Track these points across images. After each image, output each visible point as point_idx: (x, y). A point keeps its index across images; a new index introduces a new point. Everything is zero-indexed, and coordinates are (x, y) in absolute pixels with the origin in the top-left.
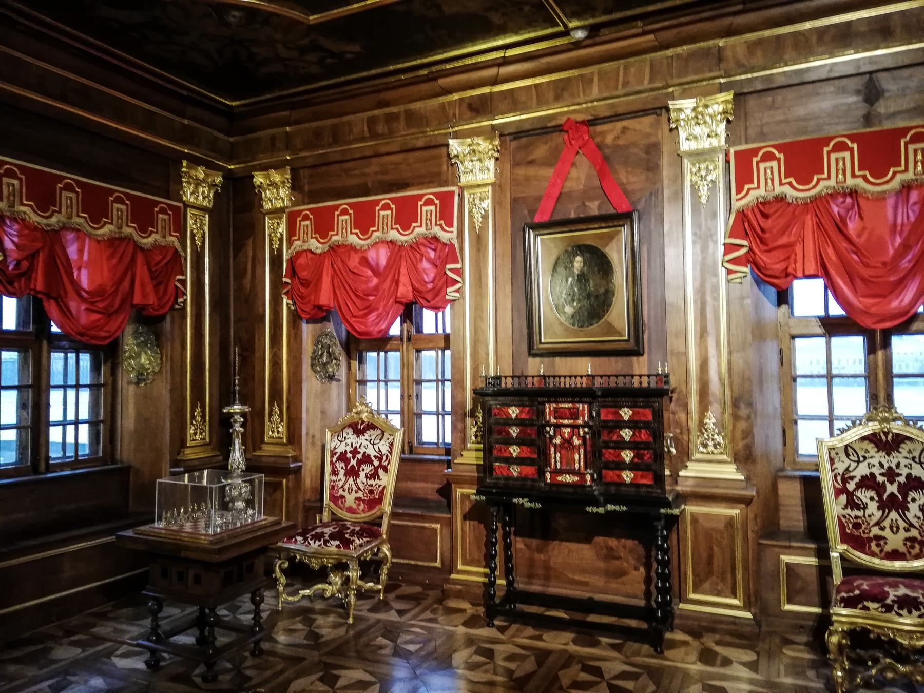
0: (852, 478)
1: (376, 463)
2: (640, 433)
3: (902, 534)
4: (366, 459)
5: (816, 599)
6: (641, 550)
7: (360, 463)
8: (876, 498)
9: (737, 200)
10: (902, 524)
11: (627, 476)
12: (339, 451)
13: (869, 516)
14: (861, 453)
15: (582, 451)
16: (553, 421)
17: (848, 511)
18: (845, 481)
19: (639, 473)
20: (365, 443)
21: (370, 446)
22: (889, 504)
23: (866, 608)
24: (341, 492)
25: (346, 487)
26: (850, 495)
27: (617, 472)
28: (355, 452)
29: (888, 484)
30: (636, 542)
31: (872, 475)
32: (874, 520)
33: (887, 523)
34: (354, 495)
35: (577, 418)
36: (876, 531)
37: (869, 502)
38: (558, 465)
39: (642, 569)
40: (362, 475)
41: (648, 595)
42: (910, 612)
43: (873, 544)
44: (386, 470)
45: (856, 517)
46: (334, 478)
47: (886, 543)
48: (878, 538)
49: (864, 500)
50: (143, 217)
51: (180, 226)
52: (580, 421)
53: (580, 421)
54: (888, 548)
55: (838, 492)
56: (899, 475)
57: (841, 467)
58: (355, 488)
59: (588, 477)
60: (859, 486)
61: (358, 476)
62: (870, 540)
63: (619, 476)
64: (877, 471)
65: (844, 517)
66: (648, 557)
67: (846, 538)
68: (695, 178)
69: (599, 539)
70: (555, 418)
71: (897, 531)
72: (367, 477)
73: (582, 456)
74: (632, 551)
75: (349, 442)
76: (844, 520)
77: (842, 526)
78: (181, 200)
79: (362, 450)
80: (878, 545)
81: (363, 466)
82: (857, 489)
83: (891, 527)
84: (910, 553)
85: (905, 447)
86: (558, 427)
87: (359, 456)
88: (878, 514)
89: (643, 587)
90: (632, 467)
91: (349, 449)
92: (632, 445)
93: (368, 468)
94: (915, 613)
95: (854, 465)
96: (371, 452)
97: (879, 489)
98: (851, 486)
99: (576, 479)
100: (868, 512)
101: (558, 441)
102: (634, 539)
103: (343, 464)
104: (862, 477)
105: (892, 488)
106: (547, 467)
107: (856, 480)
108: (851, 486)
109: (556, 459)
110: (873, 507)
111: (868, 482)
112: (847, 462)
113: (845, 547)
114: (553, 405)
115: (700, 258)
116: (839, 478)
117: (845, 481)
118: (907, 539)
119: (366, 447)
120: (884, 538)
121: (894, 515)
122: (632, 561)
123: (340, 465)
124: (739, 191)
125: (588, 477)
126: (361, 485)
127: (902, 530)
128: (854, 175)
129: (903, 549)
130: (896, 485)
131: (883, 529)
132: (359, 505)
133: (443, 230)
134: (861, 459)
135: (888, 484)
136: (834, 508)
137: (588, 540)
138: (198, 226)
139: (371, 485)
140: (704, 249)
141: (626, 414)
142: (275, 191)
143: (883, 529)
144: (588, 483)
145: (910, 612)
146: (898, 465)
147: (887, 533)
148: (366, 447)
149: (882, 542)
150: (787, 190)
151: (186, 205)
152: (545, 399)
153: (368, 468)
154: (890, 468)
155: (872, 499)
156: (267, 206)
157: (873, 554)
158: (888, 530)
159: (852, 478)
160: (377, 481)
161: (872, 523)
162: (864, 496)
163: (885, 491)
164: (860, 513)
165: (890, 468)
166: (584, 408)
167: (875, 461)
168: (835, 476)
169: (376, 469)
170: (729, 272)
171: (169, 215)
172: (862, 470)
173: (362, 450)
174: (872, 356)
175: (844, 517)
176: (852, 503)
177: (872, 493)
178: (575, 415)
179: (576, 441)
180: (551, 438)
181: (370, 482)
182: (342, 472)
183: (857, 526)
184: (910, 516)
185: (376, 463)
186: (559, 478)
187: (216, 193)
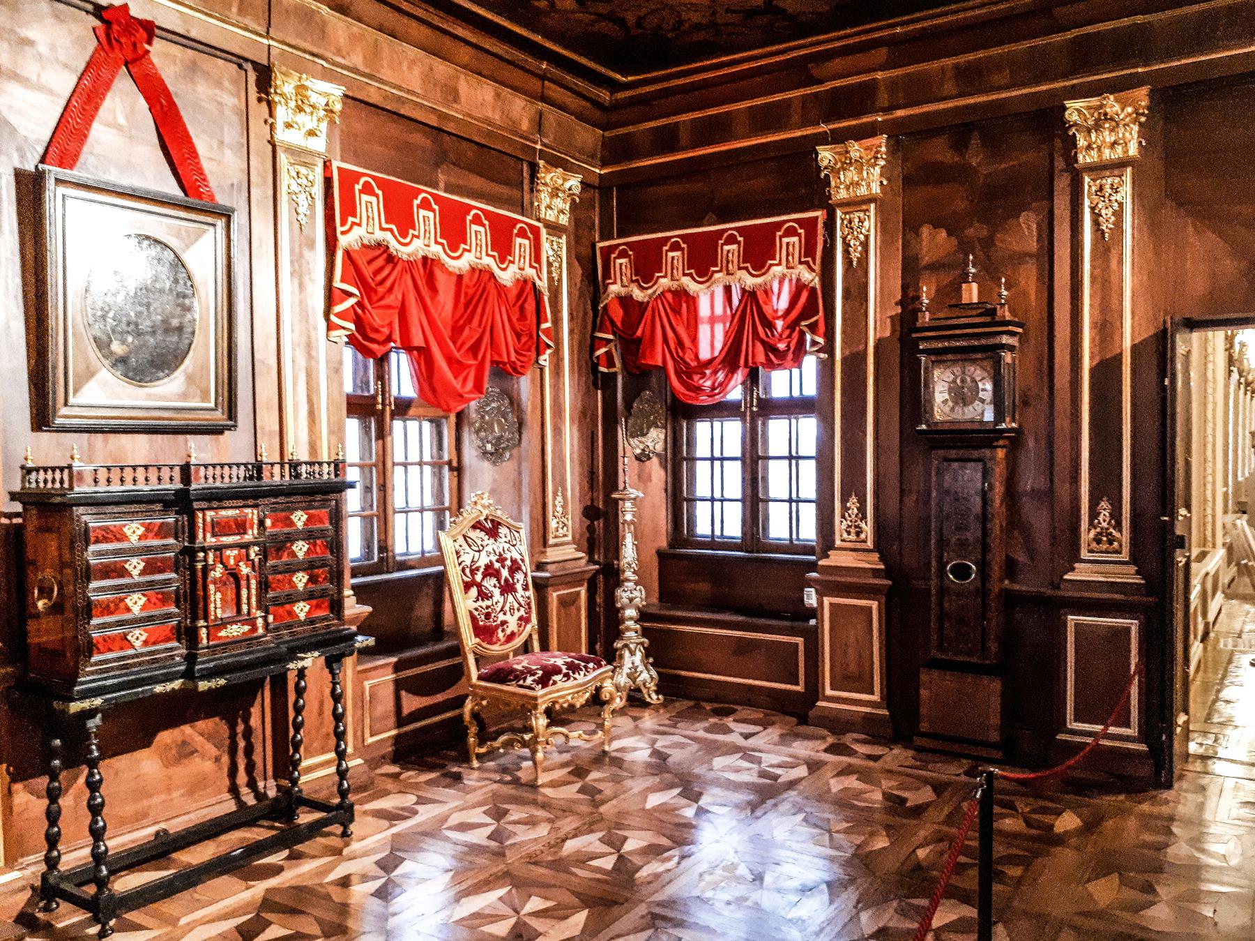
0: (478, 569)
2: (315, 545)
3: (517, 615)
5: (392, 721)
6: (224, 730)
9: (343, 233)
11: (302, 610)
14: (479, 542)
15: (253, 583)
16: (211, 540)
17: (480, 603)
18: (473, 572)
19: (314, 602)
22: (507, 588)
23: (555, 683)
26: (479, 586)
27: (288, 607)
30: (217, 719)
32: (500, 605)
33: (507, 608)
35: (245, 533)
36: (501, 617)
38: (219, 611)
39: (225, 759)
41: (234, 790)
43: (500, 630)
45: (488, 607)
48: (504, 623)
49: (491, 589)
52: (248, 537)
53: (248, 537)
54: (508, 632)
55: (467, 586)
57: (467, 559)
59: (260, 622)
60: (485, 576)
62: (497, 627)
63: (291, 613)
65: (476, 609)
66: (233, 736)
67: (479, 631)
68: (295, 188)
69: (165, 737)
70: (214, 535)
73: (253, 592)
74: (209, 737)
76: (476, 613)
77: (474, 619)
80: (503, 630)
85: (503, 531)
86: (219, 549)
88: (501, 600)
89: (227, 782)
90: (308, 596)
92: (309, 566)
97: (496, 574)
98: (478, 578)
99: (246, 628)
100: (495, 599)
101: (218, 572)
102: (208, 716)
106: (195, 618)
107: (482, 570)
108: (478, 578)
109: (217, 604)
110: (497, 592)
111: (490, 571)
113: (478, 640)
114: (210, 514)
115: (297, 301)
116: (467, 571)
117: (473, 572)
121: (510, 598)
122: (214, 751)
124: (343, 223)
125: (260, 622)
128: (436, 242)
136: (464, 604)
137: (146, 742)
140: (301, 286)
141: (299, 519)
144: (261, 631)
147: (508, 617)
150: (388, 235)
152: (204, 505)
159: (478, 569)
162: (490, 583)
164: (488, 603)
166: (252, 514)
168: (463, 570)
170: (330, 327)
172: (483, 561)
174: (380, 442)
175: (476, 609)
176: (483, 595)
177: (494, 581)
178: (241, 527)
179: (245, 570)
180: (206, 570)
183: (488, 616)
184: (518, 595)
186: (223, 633)
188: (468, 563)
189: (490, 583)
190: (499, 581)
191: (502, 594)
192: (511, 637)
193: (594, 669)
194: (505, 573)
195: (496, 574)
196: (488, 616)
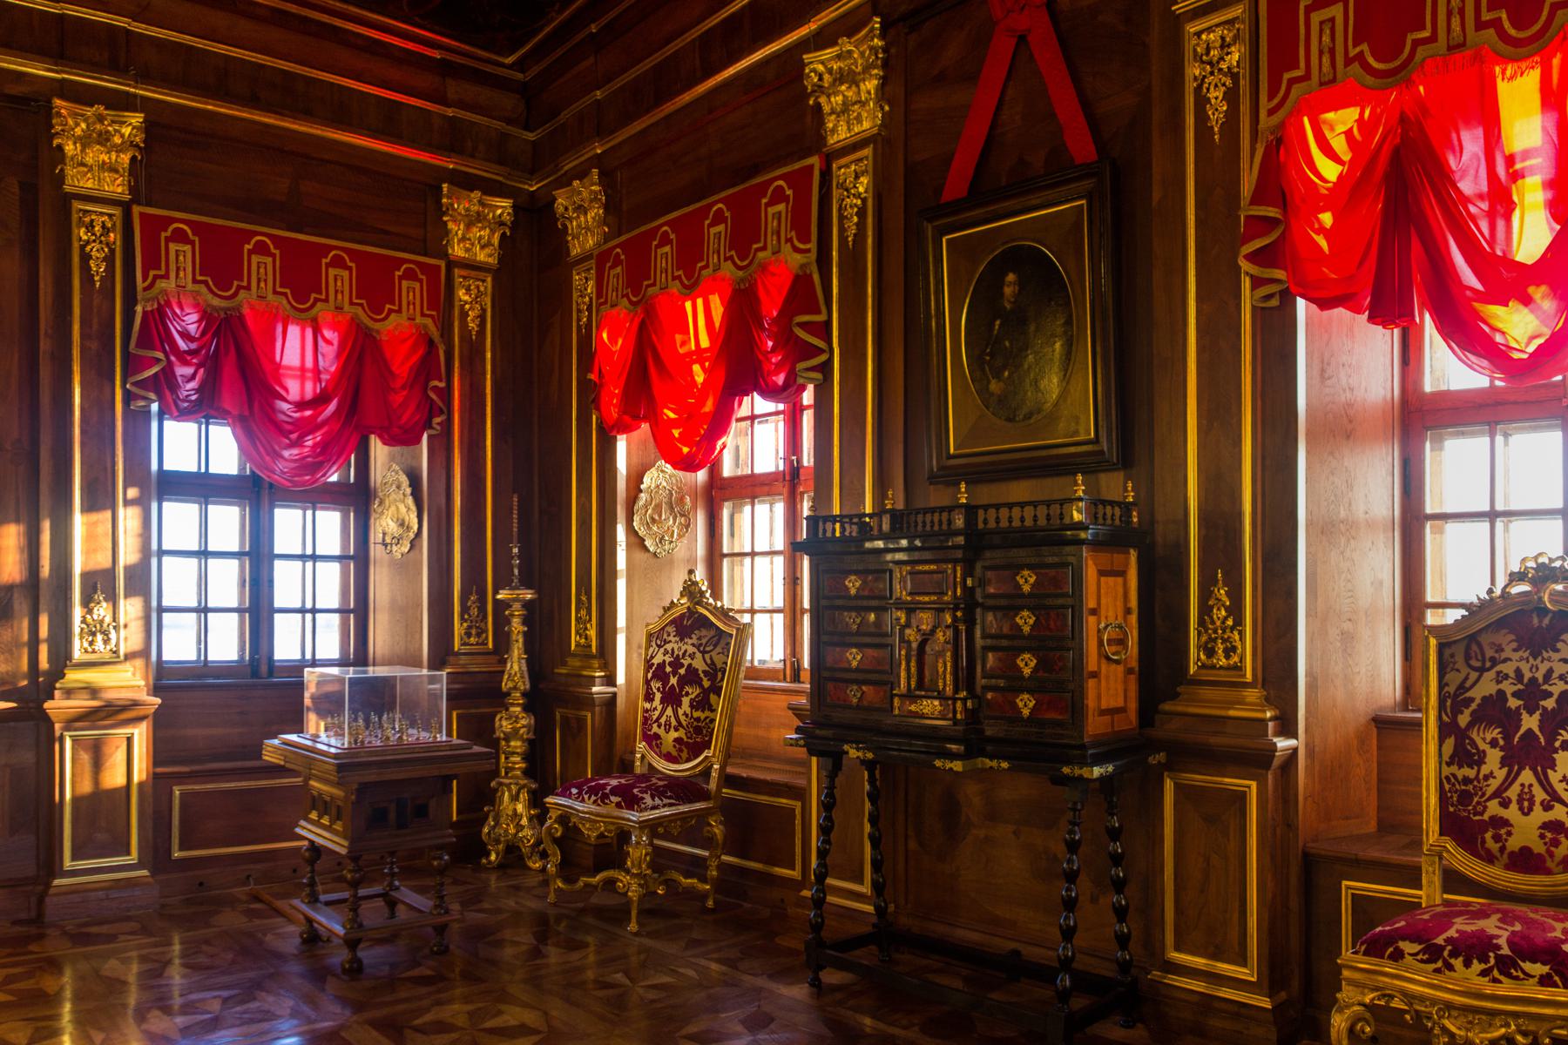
1: (706, 684)
3: (1539, 816)
4: (692, 677)
7: (683, 681)
8: (1501, 742)
10: (1540, 795)
12: (656, 661)
13: (1486, 778)
14: (1489, 653)
17: (1454, 769)
20: (691, 649)
21: (699, 655)
24: (655, 728)
25: (663, 720)
28: (676, 664)
29: (1525, 716)
31: (1501, 693)
32: (1494, 784)
33: (1513, 793)
34: (674, 735)
36: (1494, 808)
37: (1486, 747)
40: (686, 701)
42: (1467, 964)
43: (1488, 835)
44: (718, 691)
45: (1466, 780)
46: (647, 705)
47: (1509, 834)
48: (1499, 822)
49: (1482, 746)
50: (376, 289)
51: (440, 300)
54: (1514, 844)
56: (1550, 695)
57: (1454, 679)
58: (674, 722)
60: (1476, 720)
61: (680, 705)
62: (1484, 826)
64: (1508, 687)
71: (1530, 809)
72: (691, 706)
75: (669, 647)
76: (1447, 787)
78: (444, 254)
79: (686, 662)
80: (1497, 838)
81: (687, 688)
82: (1470, 725)
83: (1520, 801)
84: (1551, 855)
87: (682, 671)
88: (1501, 774)
91: (668, 659)
93: (693, 691)
94: (1477, 966)
95: (1474, 675)
96: (699, 664)
98: (1464, 719)
100: (1485, 770)
103: (659, 685)
104: (1484, 698)
105: (1530, 722)
107: (1474, 706)
108: (1464, 719)
110: (1494, 757)
111: (1495, 712)
112: (1465, 670)
117: (1456, 711)
118: (1546, 826)
119: (692, 656)
120: (1505, 823)
123: (655, 685)
126: (682, 718)
127: (1537, 808)
129: (1539, 847)
130: (1537, 716)
131: (1505, 804)
132: (681, 750)
133: (796, 250)
134: (1488, 664)
135: (1525, 716)
138: (472, 299)
139: (698, 719)
142: (584, 220)
143: (1505, 804)
145: (1467, 964)
146: (1548, 676)
148: (692, 656)
149: (1503, 831)
151: (452, 264)
153: (693, 691)
154: (1533, 680)
155: (1494, 743)
156: (576, 251)
157: (1490, 858)
158: (1514, 806)
160: (707, 713)
161: (1488, 794)
163: (1519, 727)
164: (1471, 773)
165: (1533, 680)
167: (1508, 668)
169: (706, 693)
171: (421, 281)
172: (1486, 687)
173: (686, 662)
181: (696, 714)
182: (658, 696)
185: (706, 684)
187: (503, 235)
188: (1451, 689)
189: (1483, 738)
190: (1508, 737)
191: (1504, 762)
192: (1525, 861)
193: (1545, 981)
194: (1530, 722)
195: (1509, 721)
196: (1465, 797)
